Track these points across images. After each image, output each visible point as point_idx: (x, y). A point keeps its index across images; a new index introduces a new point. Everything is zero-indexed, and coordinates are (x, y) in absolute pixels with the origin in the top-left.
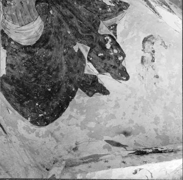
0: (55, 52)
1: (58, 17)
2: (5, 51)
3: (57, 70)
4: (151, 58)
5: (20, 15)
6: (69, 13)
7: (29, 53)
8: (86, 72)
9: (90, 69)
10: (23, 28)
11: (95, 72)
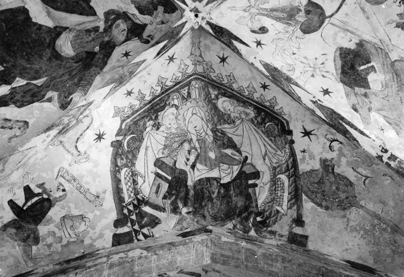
0: (46, 62)
1: (74, 66)
2: (53, 27)
3: (28, 60)
4: (6, 126)
5: (79, 41)
6: (74, 73)
7: (49, 45)
8: (17, 79)
9: (20, 82)
10: (69, 43)
11: (14, 85)
